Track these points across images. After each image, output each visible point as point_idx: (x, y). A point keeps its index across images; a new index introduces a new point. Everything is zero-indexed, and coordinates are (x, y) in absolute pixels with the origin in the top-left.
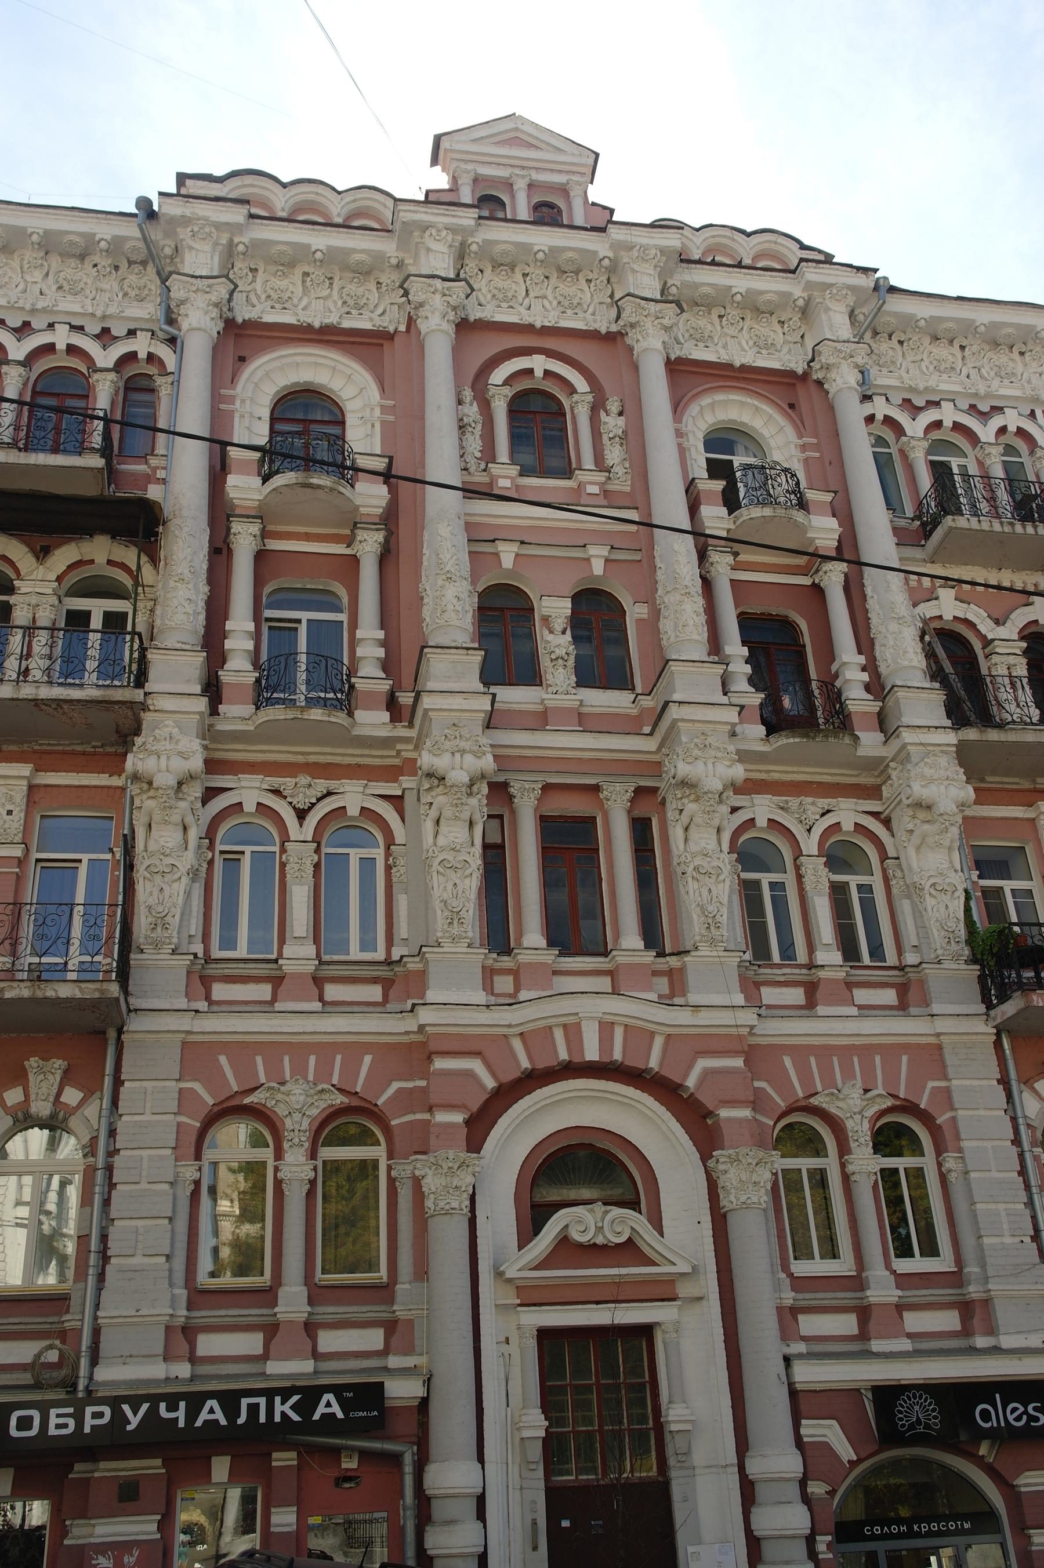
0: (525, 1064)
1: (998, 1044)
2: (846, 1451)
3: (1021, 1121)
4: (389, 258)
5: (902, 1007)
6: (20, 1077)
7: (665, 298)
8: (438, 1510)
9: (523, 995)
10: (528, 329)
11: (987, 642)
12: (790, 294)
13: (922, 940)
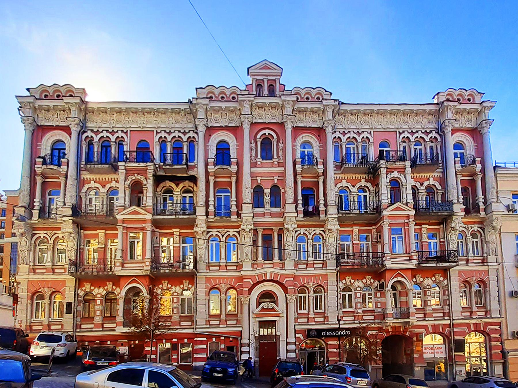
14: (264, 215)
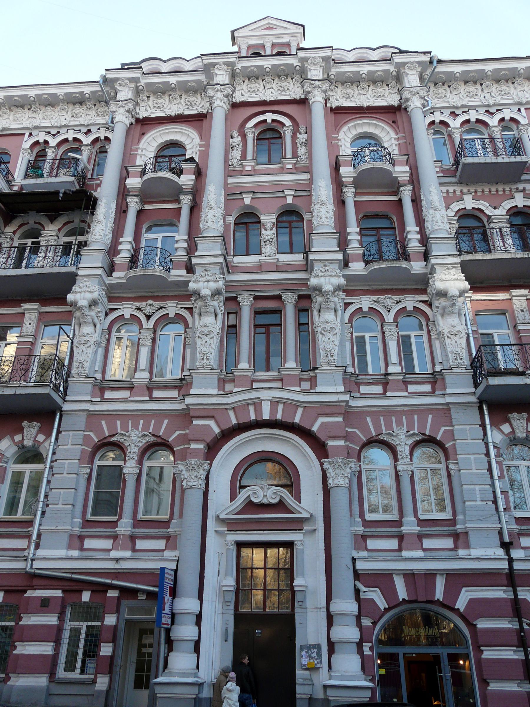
0: (234, 421)
3: (491, 444)
4: (203, 82)
5: (433, 393)
6: (21, 430)
7: (327, 79)
10: (264, 103)
11: (489, 217)
12: (389, 70)
13: (444, 359)
14: (260, 269)
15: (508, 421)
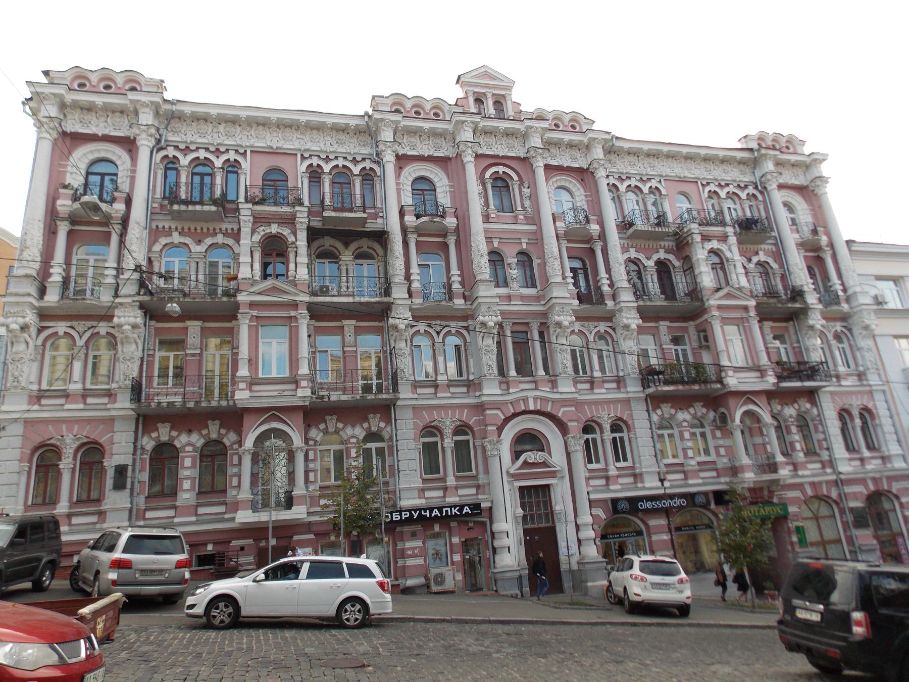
1: (646, 400)
2: (603, 516)
6: (366, 419)
8: (496, 535)
9: (511, 390)
11: (645, 267)
15: (660, 407)
